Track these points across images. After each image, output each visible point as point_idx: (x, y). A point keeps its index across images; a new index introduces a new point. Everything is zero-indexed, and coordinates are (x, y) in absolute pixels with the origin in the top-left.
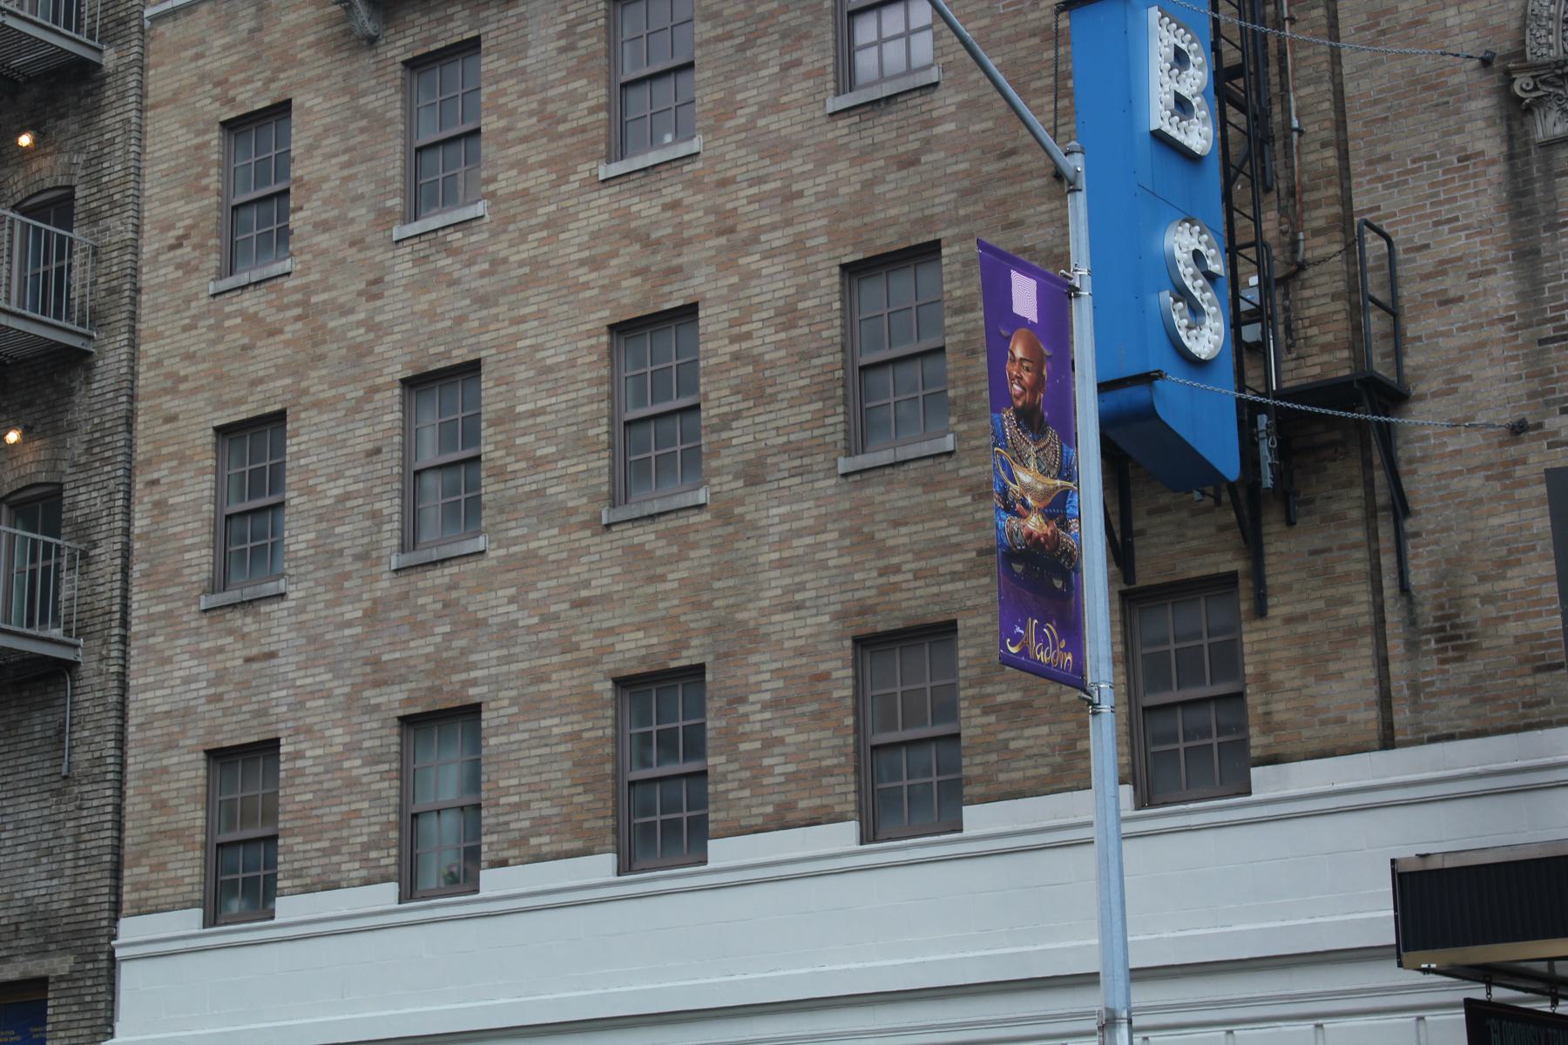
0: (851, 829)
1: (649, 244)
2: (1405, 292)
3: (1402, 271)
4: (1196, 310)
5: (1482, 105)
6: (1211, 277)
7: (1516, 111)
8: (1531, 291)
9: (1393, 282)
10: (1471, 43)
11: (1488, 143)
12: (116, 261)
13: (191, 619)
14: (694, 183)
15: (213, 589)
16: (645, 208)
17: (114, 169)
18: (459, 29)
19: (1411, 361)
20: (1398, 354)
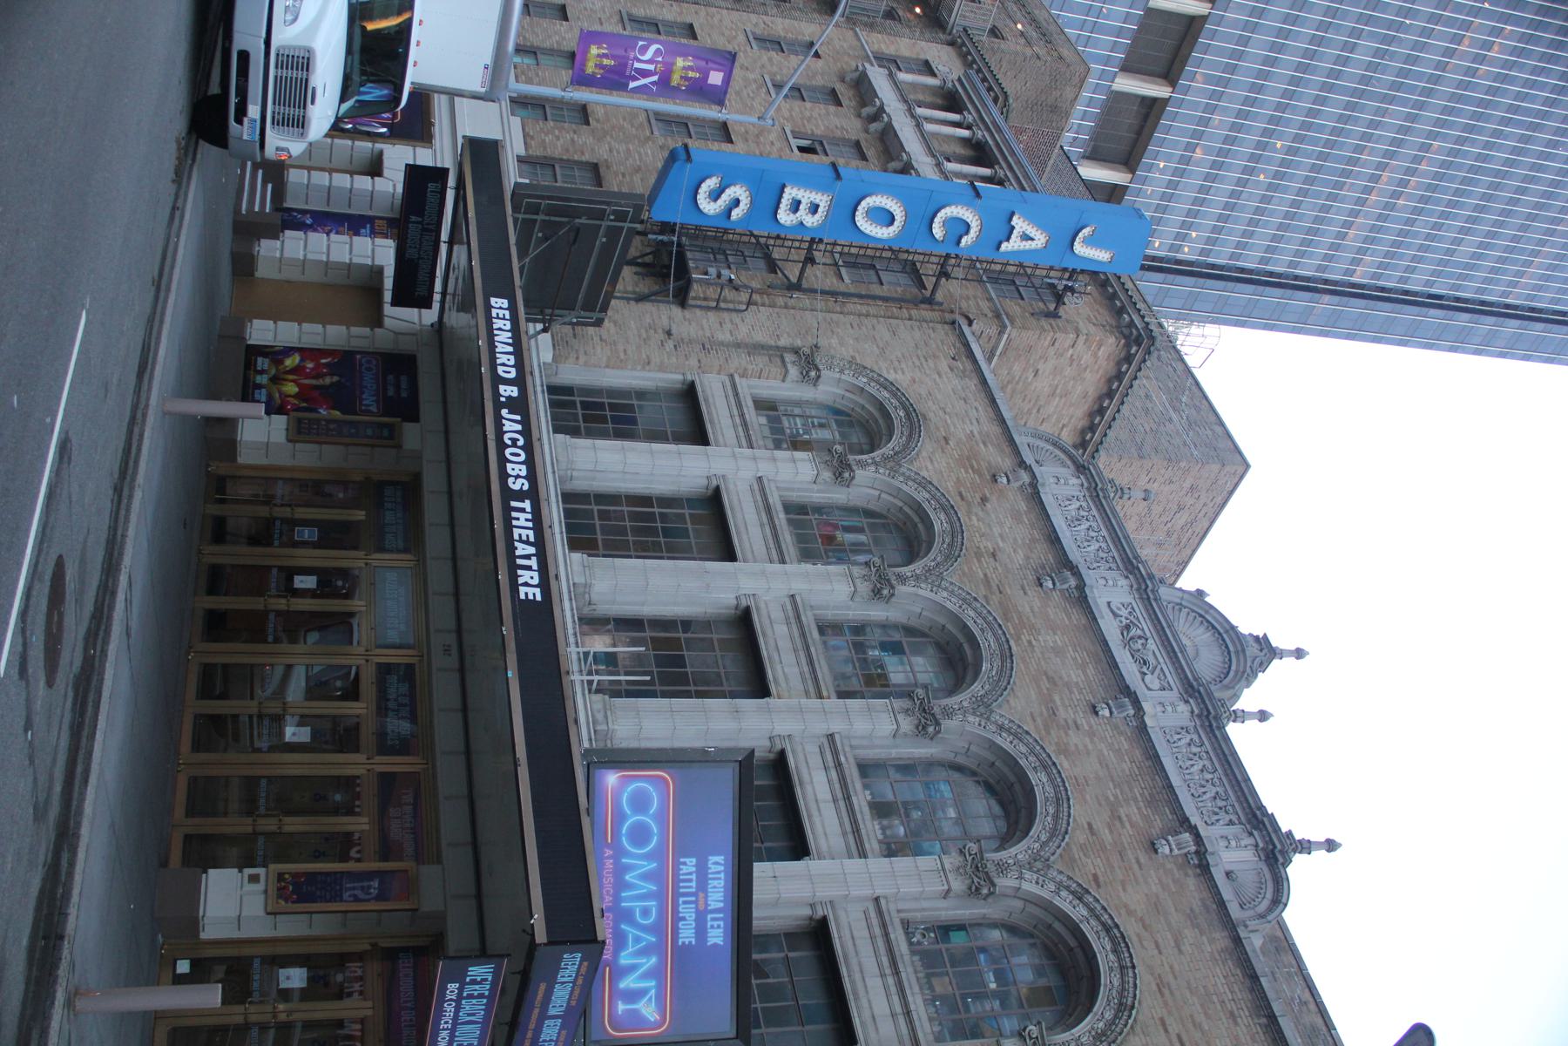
0: (522, 152)
1: (757, 136)
2: (726, 315)
3: (734, 315)
4: (715, 195)
5: (799, 343)
6: (729, 211)
7: (796, 351)
8: (722, 344)
9: (728, 310)
10: (822, 342)
11: (783, 342)
12: (762, 9)
13: (619, 7)
14: (781, 150)
15: (629, 15)
16: (772, 137)
17: (797, 14)
18: (845, 102)
19: (698, 312)
20: (700, 307)
